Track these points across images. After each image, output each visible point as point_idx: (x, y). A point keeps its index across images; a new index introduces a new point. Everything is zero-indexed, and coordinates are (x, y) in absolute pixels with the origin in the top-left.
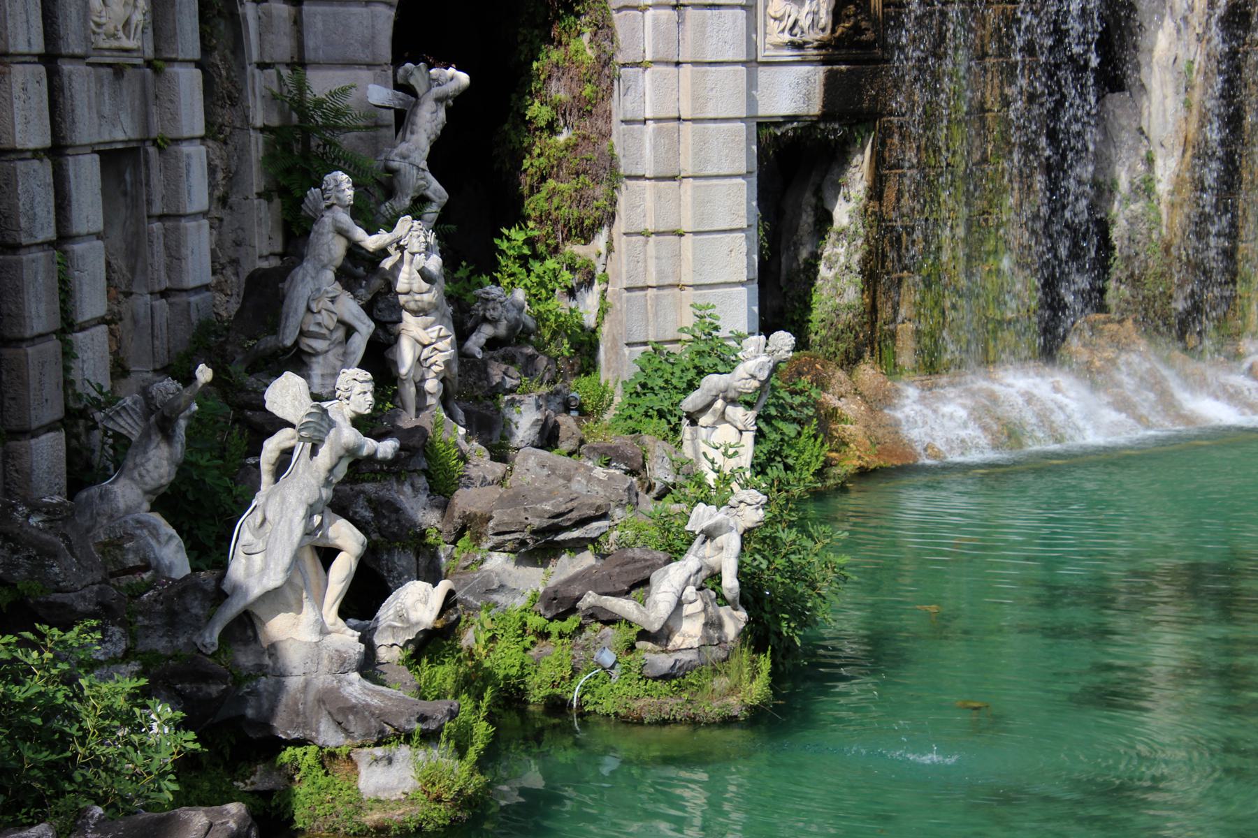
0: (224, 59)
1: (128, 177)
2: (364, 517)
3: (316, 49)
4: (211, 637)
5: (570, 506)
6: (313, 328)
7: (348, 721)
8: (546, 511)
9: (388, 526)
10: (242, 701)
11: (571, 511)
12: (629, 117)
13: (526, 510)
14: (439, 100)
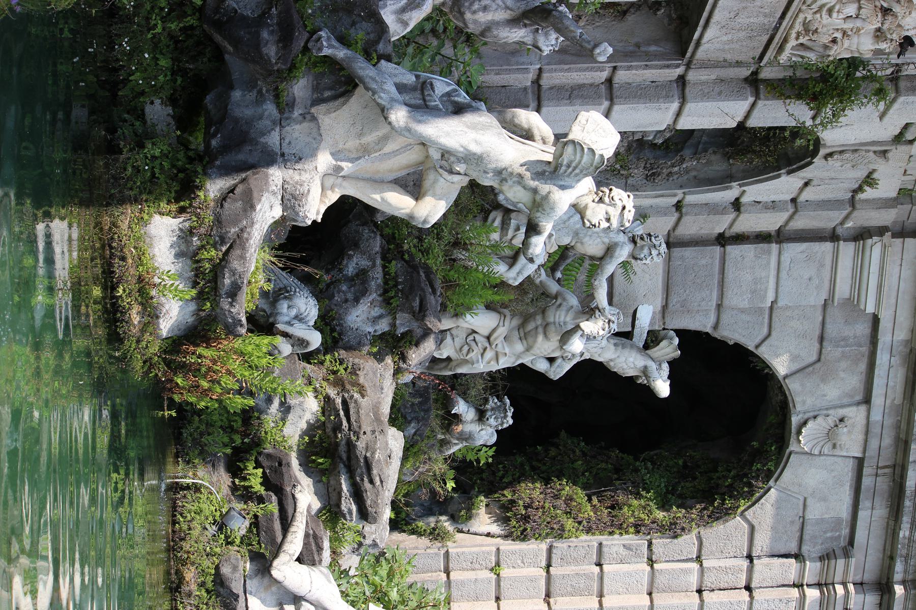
0: (687, 171)
1: (653, 48)
2: (347, 266)
3: (682, 257)
4: (330, 48)
5: (377, 481)
6: (513, 223)
7: (235, 200)
8: (373, 453)
9: (339, 291)
10: (251, 85)
11: (371, 482)
12: (605, 549)
13: (373, 432)
14: (645, 371)
